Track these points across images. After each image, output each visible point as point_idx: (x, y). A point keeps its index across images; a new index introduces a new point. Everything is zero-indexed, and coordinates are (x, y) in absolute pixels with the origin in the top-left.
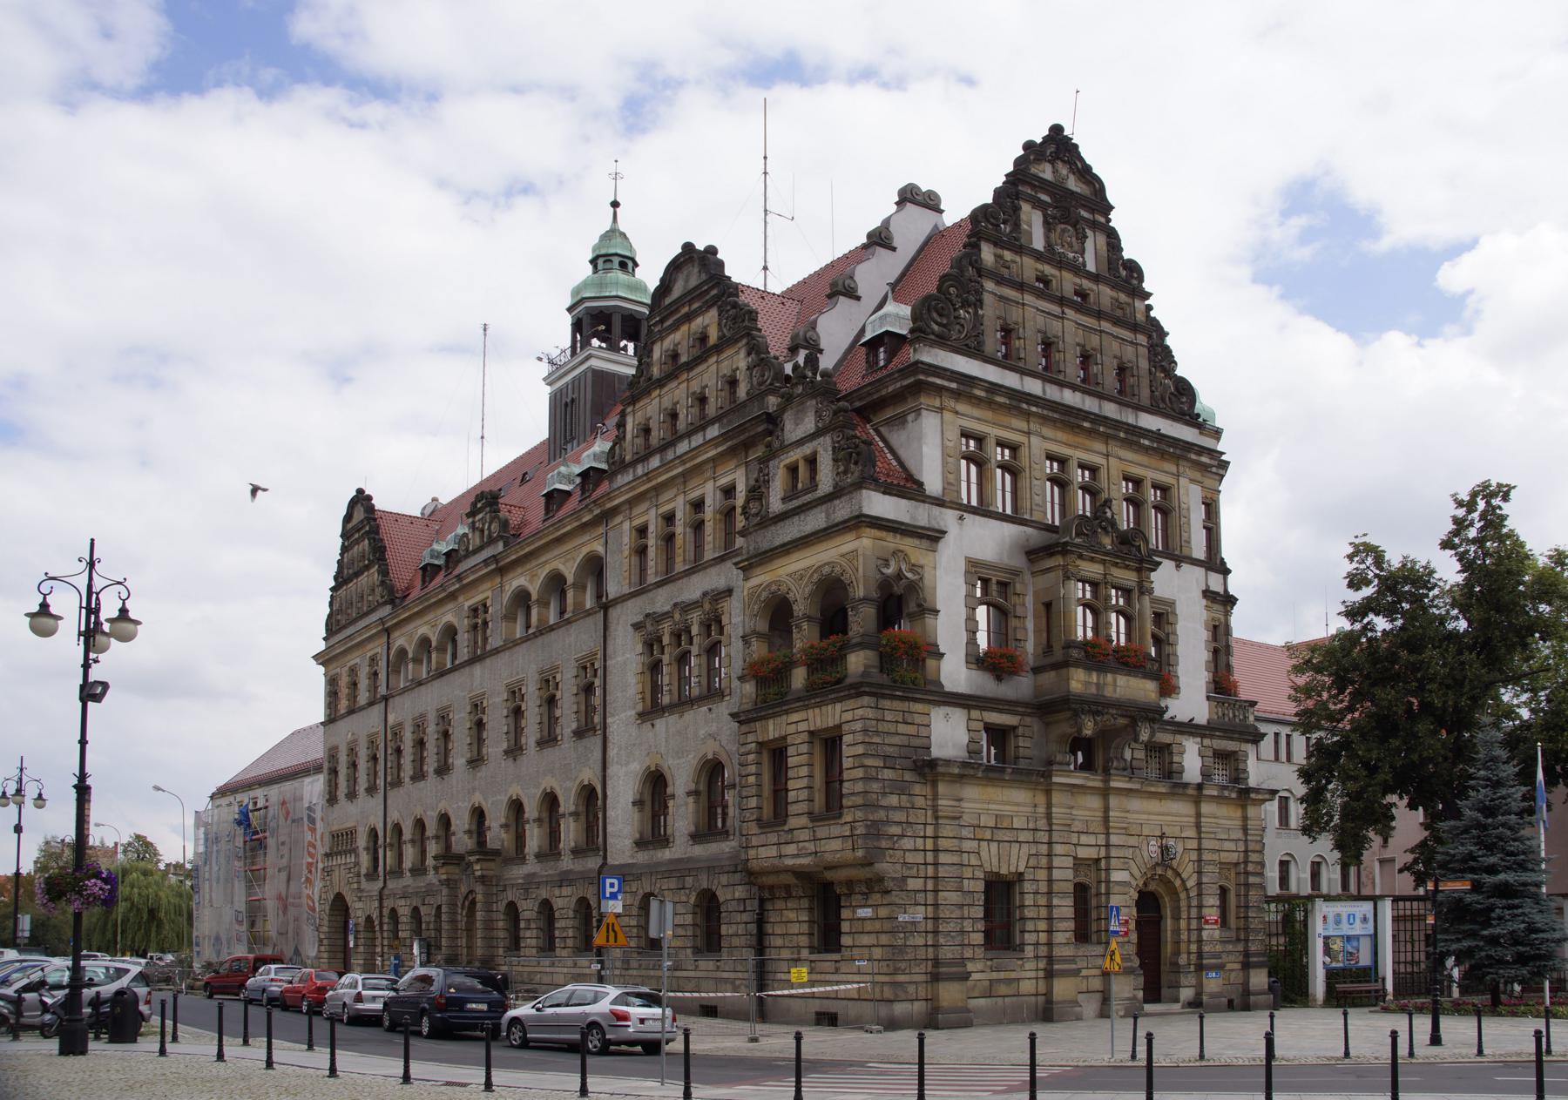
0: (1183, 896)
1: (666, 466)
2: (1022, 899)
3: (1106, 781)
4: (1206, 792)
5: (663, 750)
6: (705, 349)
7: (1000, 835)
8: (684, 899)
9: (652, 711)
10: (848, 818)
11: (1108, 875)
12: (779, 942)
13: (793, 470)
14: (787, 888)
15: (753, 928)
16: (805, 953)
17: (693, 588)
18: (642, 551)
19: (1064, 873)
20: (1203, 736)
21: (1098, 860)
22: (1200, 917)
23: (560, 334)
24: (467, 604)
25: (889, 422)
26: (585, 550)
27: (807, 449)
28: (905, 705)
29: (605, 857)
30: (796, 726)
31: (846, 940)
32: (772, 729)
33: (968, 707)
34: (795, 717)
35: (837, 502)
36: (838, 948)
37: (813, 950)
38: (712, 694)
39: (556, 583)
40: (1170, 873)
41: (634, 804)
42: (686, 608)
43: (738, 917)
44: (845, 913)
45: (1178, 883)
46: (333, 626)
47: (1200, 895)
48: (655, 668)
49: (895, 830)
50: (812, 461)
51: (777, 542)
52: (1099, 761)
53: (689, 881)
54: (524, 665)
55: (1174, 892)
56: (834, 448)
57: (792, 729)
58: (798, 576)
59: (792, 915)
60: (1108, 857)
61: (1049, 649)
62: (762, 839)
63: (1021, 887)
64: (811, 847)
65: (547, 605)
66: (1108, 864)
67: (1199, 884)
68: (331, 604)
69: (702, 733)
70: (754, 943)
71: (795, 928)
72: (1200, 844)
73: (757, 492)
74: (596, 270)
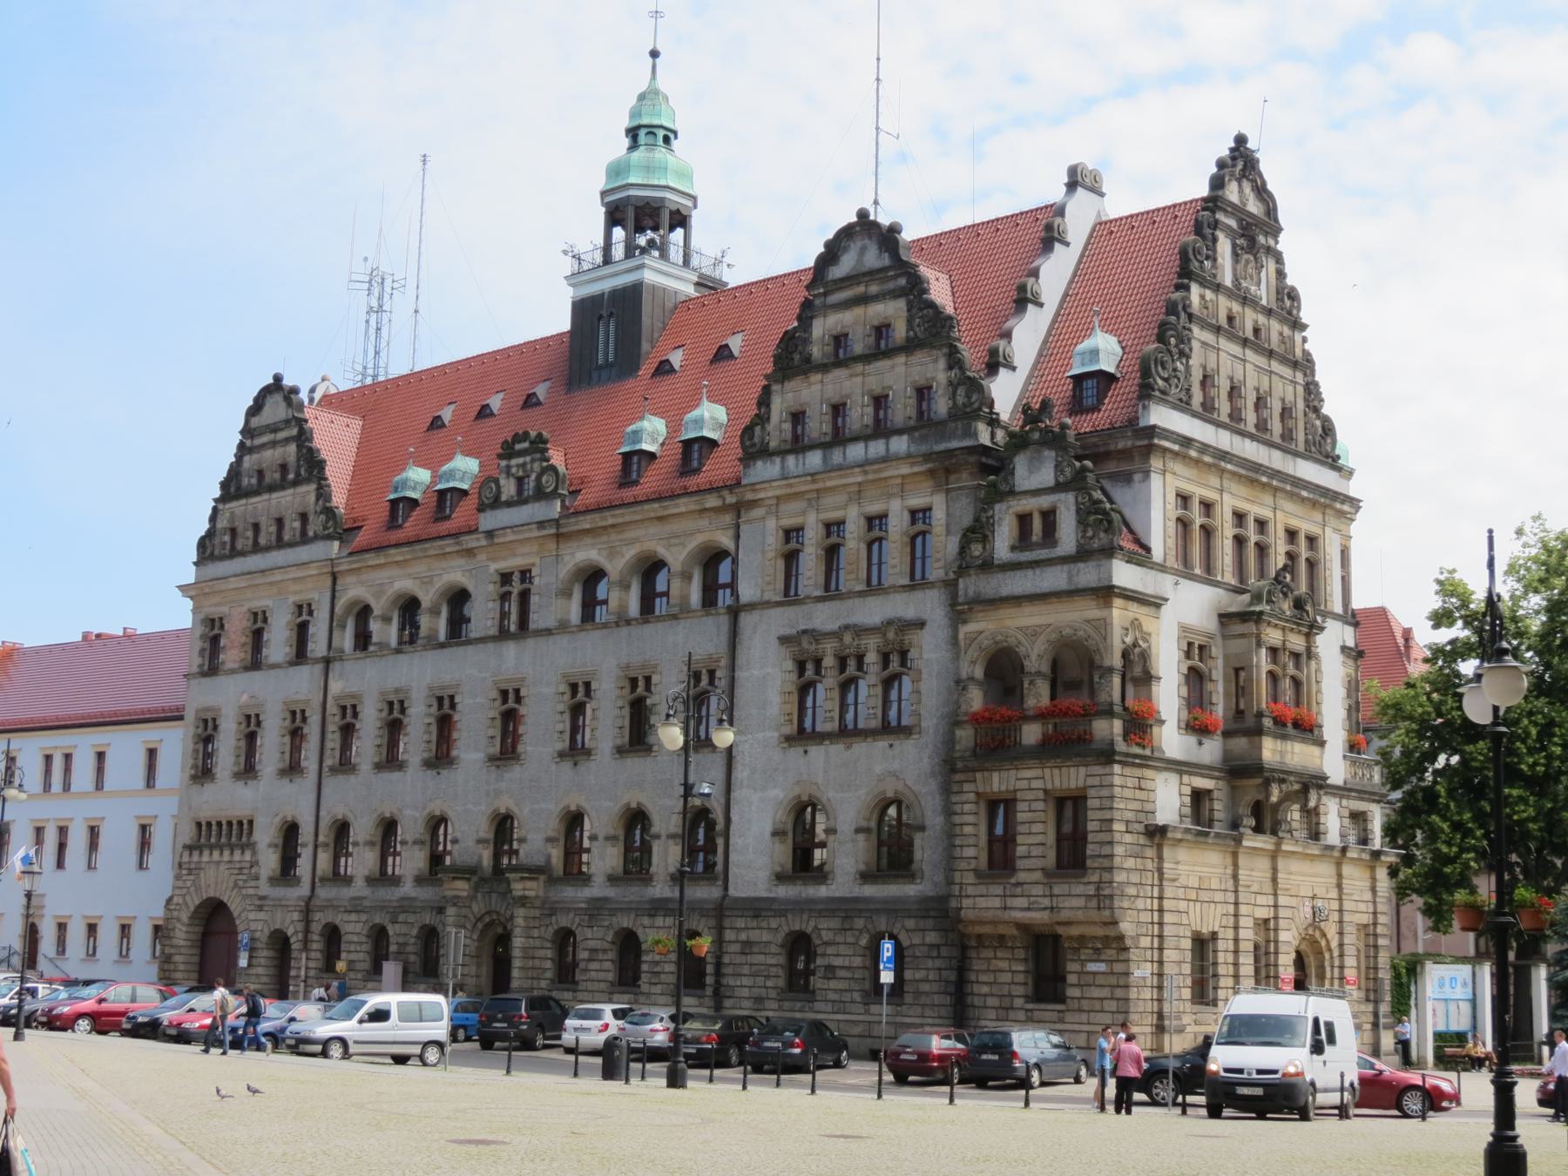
0: (1327, 956)
1: (829, 469)
2: (1216, 957)
3: (1278, 845)
4: (1349, 854)
5: (820, 781)
6: (882, 346)
7: (1204, 896)
8: (851, 940)
9: (802, 735)
10: (1095, 878)
11: (1276, 935)
12: (985, 989)
13: (1024, 520)
14: (1002, 938)
15: (952, 976)
16: (1019, 1002)
17: (872, 612)
18: (791, 558)
19: (1248, 934)
20: (1341, 797)
21: (1266, 921)
22: (1342, 978)
23: (587, 228)
24: (494, 567)
25: (1112, 477)
26: (700, 539)
27: (1045, 501)
28: (1138, 772)
29: (726, 889)
30: (1030, 783)
31: (1072, 992)
32: (998, 782)
33: (1181, 773)
34: (1028, 774)
35: (1081, 565)
36: (1061, 999)
37: (1028, 999)
38: (889, 729)
39: (651, 568)
40: (1317, 934)
41: (775, 834)
42: (860, 631)
43: (930, 963)
44: (1072, 966)
45: (1323, 943)
46: (207, 550)
47: (1341, 955)
48: (805, 689)
49: (1132, 891)
50: (1049, 517)
51: (1005, 591)
52: (1268, 824)
53: (859, 923)
54: (603, 658)
55: (1319, 953)
56: (1078, 511)
57: (1023, 784)
58: (1032, 633)
59: (1004, 965)
60: (1276, 918)
61: (1239, 713)
62: (982, 889)
63: (1215, 945)
64: (1046, 902)
65: (626, 587)
66: (1277, 924)
67: (1341, 945)
68: (213, 519)
69: (878, 769)
70: (952, 989)
71: (1007, 977)
72: (1341, 905)
73: (979, 531)
74: (634, 145)
